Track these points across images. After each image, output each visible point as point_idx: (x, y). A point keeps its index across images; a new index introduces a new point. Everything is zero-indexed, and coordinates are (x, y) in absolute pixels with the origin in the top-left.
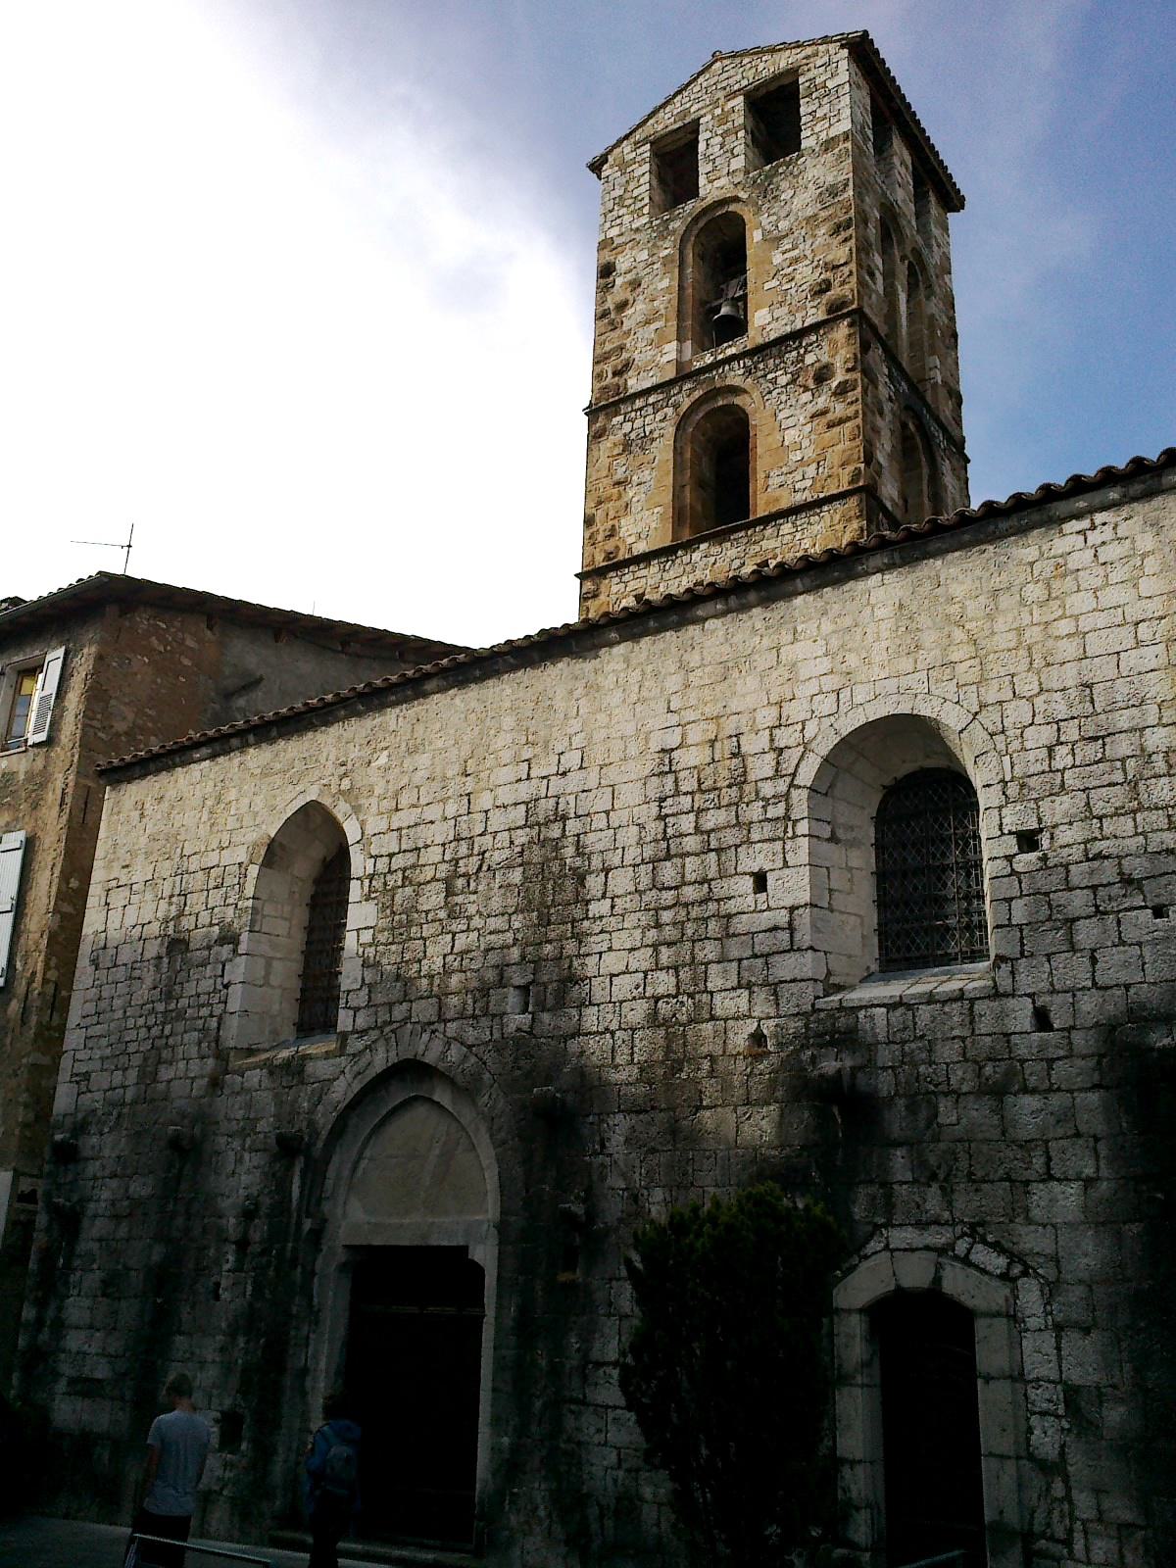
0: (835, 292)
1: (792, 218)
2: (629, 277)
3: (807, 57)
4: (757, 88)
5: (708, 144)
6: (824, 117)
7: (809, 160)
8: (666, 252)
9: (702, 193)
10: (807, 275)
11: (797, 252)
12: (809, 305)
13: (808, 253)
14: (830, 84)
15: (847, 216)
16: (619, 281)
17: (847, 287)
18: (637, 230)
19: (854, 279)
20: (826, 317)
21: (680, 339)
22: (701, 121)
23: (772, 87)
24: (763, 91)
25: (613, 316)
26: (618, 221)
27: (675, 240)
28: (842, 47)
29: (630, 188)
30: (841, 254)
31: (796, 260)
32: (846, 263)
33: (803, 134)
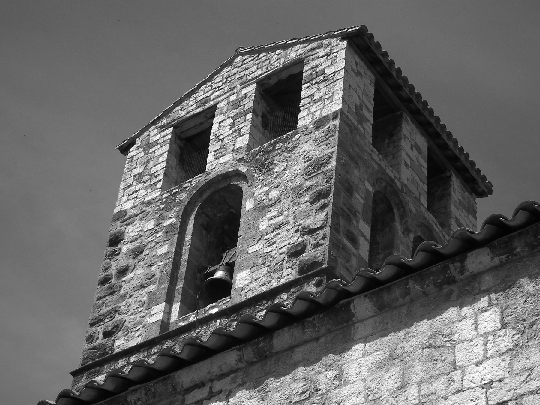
0: (306, 256)
1: (282, 187)
2: (136, 244)
3: (313, 49)
4: (268, 77)
5: (220, 126)
6: (321, 99)
7: (303, 136)
8: (170, 221)
9: (208, 167)
10: (288, 238)
11: (282, 217)
12: (286, 265)
13: (290, 219)
14: (328, 71)
15: (328, 185)
16: (125, 249)
17: (320, 248)
18: (149, 203)
19: (326, 243)
20: (298, 277)
21: (170, 301)
22: (218, 106)
23: (284, 75)
24: (273, 82)
25: (113, 281)
26: (134, 196)
27: (179, 211)
28: (343, 39)
29: (149, 166)
30: (318, 219)
31: (280, 226)
32: (321, 228)
33: (301, 115)
